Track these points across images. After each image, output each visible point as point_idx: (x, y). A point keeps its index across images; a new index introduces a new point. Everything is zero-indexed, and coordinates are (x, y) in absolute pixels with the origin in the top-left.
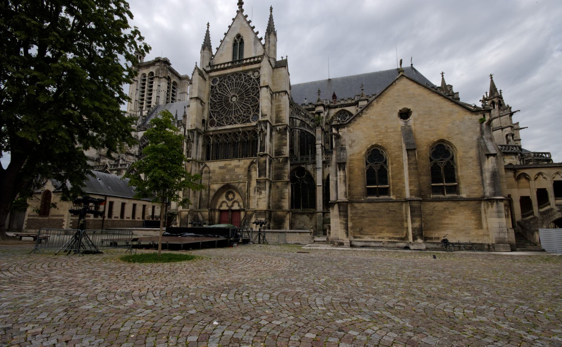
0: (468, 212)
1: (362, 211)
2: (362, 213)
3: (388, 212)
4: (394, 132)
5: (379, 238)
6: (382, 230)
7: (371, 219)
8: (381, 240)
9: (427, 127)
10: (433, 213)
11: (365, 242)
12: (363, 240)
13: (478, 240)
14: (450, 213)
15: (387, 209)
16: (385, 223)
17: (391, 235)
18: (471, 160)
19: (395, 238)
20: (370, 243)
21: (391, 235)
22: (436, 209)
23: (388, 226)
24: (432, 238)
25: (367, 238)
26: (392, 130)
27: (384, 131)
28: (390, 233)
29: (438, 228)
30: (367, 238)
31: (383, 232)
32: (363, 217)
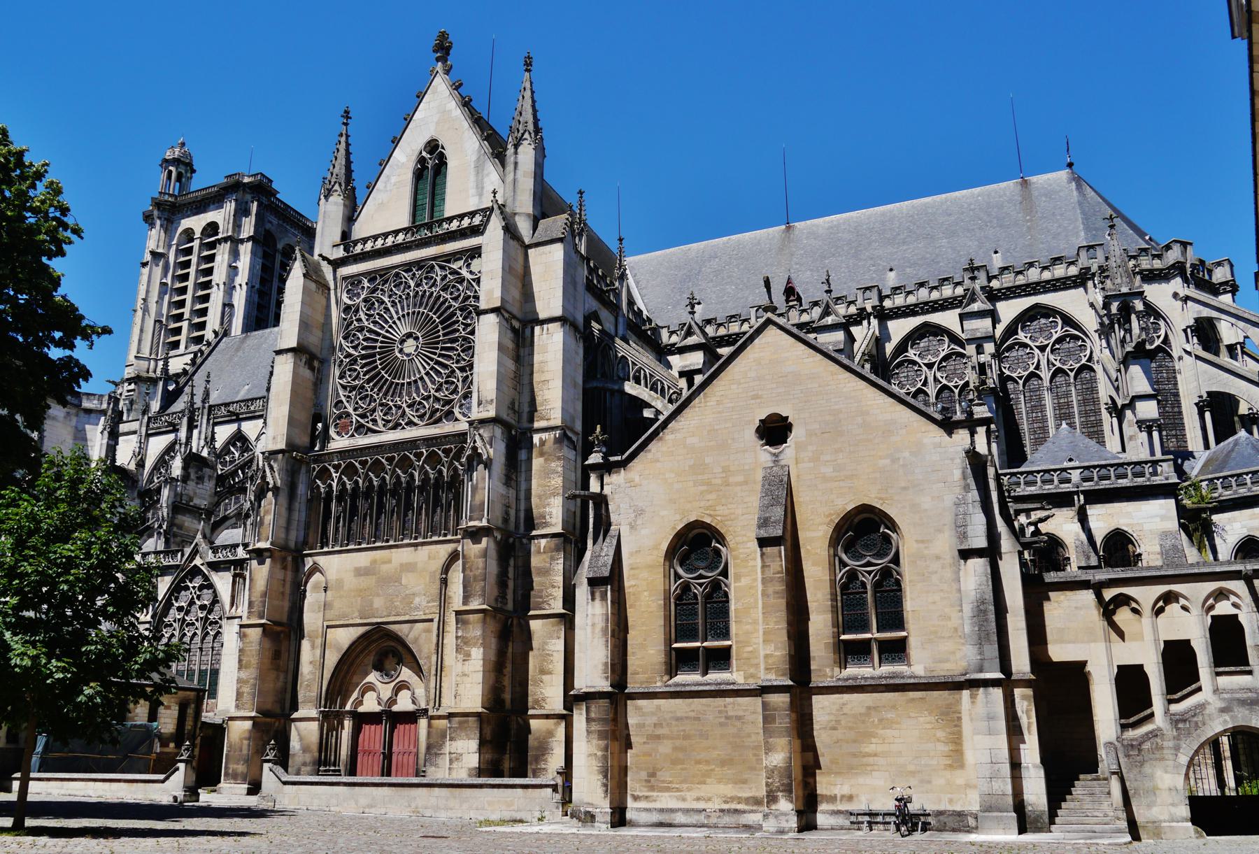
0: (929, 719)
1: (654, 719)
2: (655, 725)
3: (723, 720)
4: (746, 483)
5: (698, 799)
6: (707, 774)
7: (678, 743)
8: (701, 805)
9: (828, 470)
10: (838, 722)
11: (662, 811)
12: (658, 805)
13: (951, 801)
14: (881, 720)
15: (720, 712)
16: (715, 754)
17: (729, 790)
18: (935, 566)
19: (740, 800)
20: (673, 815)
21: (729, 790)
22: (845, 710)
23: (723, 763)
24: (835, 796)
25: (666, 800)
26: (740, 478)
27: (719, 481)
28: (727, 784)
29: (851, 768)
30: (666, 800)
31: (708, 780)
32: (658, 737)
